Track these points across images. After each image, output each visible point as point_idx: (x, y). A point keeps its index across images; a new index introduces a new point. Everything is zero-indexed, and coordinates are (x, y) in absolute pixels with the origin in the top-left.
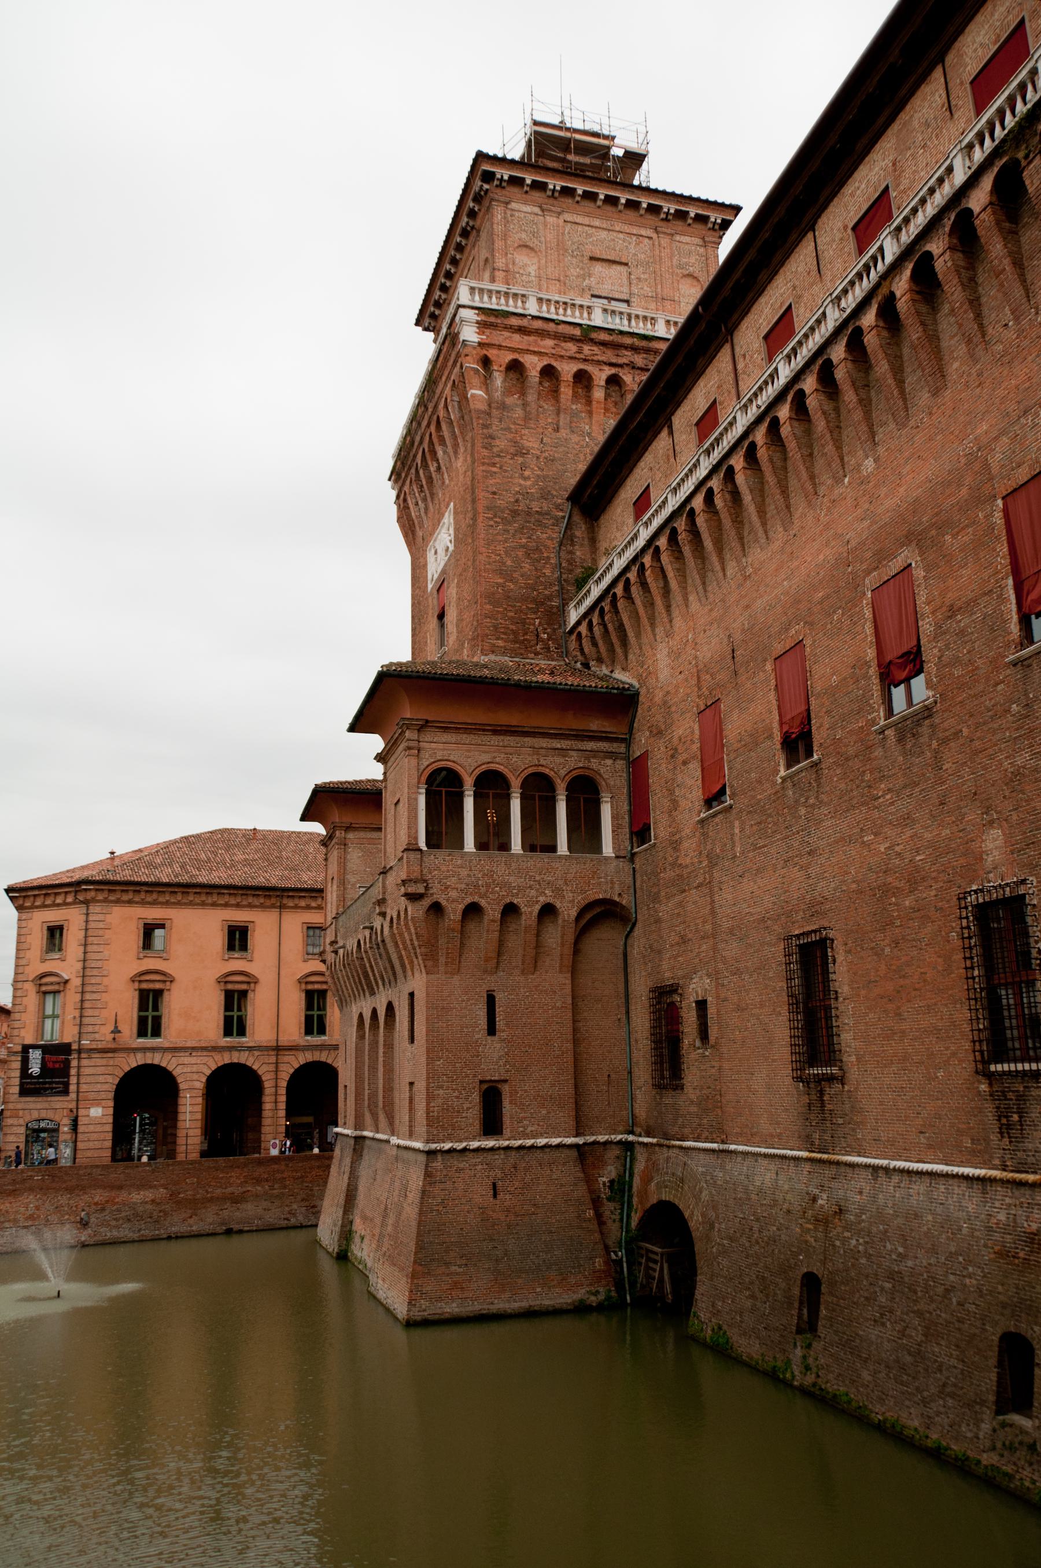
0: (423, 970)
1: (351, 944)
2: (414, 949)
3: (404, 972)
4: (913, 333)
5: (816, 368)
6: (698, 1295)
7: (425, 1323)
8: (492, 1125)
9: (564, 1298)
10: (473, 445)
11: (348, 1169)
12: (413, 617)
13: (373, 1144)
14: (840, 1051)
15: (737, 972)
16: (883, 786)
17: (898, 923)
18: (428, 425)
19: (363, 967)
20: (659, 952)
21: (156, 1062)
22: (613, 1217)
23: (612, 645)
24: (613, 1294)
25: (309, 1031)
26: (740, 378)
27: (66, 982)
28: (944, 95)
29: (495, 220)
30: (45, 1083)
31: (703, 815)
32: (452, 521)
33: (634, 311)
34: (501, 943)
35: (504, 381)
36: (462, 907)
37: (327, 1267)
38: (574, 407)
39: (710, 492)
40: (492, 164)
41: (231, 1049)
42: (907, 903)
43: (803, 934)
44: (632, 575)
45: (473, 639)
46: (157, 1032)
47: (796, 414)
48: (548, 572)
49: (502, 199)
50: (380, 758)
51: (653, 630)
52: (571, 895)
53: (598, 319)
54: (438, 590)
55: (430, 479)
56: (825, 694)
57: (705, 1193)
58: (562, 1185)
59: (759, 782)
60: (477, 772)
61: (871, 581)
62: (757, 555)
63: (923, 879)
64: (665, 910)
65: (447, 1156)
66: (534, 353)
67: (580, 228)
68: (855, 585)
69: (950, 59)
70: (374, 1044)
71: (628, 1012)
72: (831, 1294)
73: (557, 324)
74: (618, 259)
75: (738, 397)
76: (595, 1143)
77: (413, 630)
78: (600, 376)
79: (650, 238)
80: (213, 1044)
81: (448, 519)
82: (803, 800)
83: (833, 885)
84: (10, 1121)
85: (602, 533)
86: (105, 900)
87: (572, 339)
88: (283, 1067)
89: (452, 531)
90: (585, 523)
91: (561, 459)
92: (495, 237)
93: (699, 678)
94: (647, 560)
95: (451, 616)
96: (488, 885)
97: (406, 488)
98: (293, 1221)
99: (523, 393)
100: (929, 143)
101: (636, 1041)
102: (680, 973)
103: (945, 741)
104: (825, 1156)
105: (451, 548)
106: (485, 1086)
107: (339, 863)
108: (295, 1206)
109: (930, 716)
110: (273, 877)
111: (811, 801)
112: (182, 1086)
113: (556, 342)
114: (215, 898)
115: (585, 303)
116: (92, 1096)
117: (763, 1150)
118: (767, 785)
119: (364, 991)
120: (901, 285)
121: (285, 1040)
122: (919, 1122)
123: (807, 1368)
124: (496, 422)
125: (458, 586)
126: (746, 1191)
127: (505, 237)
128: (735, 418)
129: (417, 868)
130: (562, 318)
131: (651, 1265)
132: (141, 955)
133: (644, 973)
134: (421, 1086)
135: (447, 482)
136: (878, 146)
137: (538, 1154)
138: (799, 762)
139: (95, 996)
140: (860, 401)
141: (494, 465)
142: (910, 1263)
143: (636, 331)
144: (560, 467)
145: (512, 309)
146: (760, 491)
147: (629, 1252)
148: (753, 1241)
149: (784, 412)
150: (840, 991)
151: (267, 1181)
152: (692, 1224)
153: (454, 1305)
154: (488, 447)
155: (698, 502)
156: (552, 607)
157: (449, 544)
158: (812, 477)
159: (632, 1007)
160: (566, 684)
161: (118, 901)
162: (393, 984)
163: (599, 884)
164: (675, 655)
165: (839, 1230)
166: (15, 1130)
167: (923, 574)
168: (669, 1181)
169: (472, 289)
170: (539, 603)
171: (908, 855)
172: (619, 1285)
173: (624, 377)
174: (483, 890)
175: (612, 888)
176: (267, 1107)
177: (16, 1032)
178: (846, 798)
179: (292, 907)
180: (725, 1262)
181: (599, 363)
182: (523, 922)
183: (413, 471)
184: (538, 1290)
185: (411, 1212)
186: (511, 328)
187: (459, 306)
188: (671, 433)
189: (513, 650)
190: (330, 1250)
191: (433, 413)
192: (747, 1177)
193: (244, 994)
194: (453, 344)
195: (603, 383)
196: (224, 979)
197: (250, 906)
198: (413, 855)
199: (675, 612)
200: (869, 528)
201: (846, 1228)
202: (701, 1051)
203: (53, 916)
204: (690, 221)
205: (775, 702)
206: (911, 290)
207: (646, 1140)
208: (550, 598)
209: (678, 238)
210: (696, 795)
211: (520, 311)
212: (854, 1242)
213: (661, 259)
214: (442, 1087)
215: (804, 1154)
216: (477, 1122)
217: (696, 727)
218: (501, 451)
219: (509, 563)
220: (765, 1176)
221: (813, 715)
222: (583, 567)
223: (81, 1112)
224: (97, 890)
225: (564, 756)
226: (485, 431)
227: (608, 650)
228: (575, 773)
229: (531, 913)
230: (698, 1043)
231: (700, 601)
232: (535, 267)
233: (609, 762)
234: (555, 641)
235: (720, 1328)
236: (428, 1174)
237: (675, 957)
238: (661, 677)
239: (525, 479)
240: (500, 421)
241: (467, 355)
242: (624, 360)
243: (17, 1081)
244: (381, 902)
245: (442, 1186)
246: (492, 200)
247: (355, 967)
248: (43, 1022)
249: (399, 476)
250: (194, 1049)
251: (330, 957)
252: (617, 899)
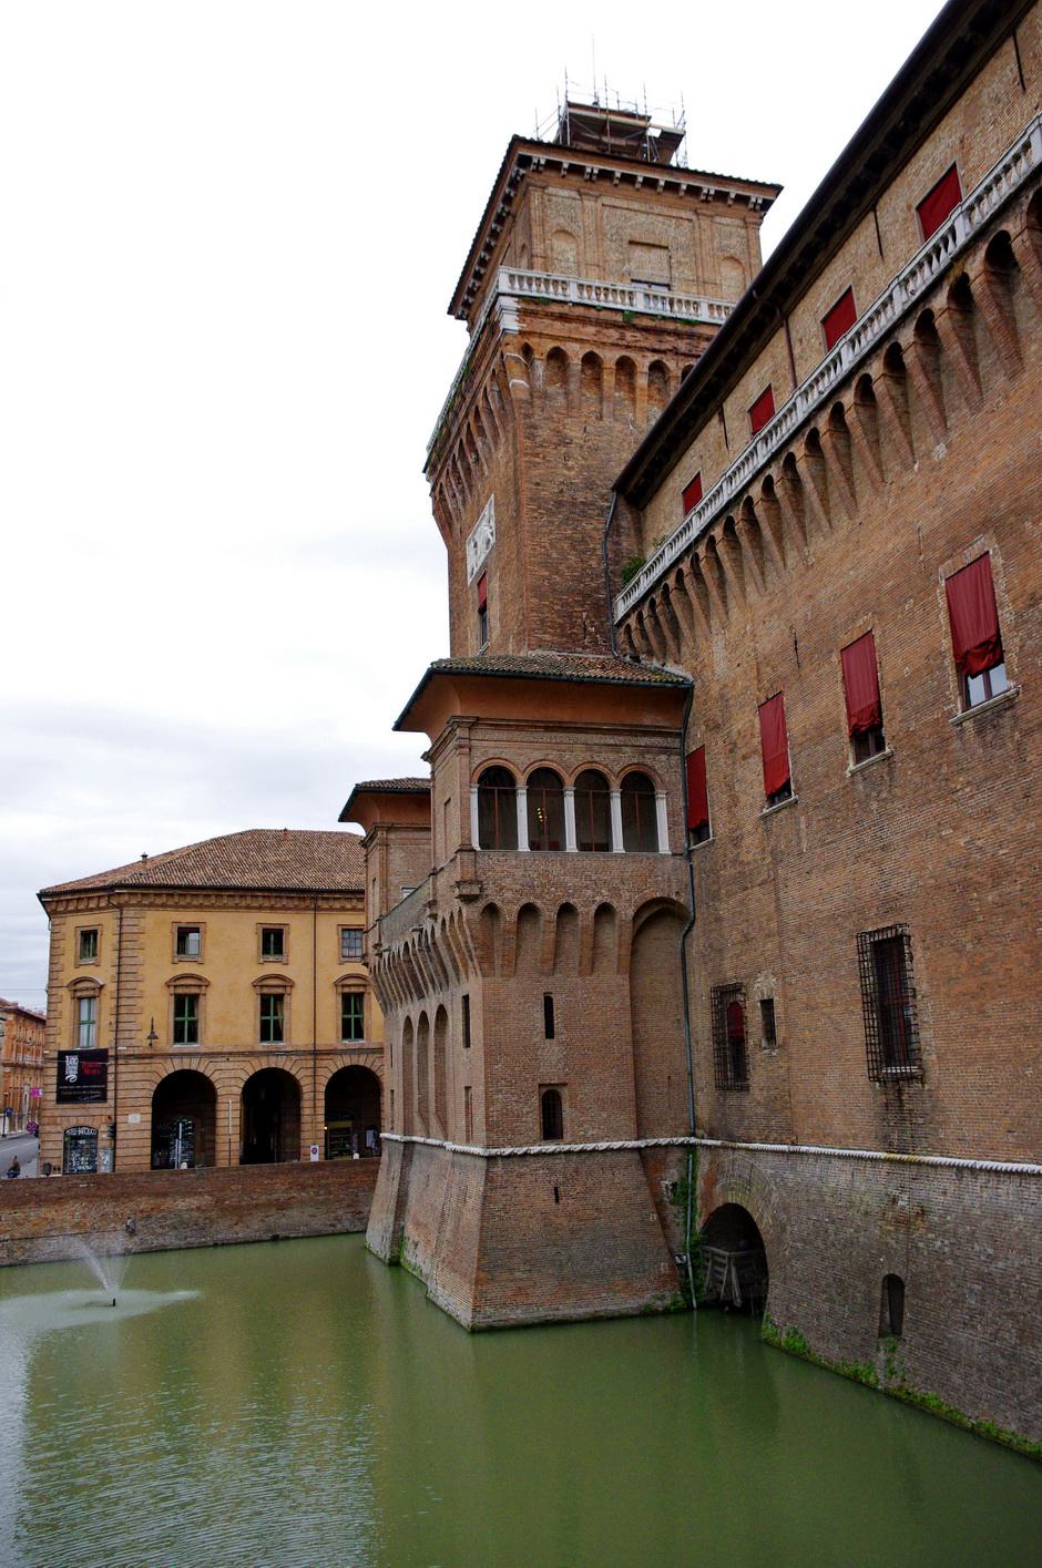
0: (479, 972)
1: (398, 946)
2: (469, 951)
3: (457, 975)
4: (988, 315)
5: (883, 352)
6: (770, 1299)
7: (491, 1330)
8: (552, 1130)
9: (631, 1304)
10: (515, 435)
11: (397, 1175)
12: (451, 611)
13: (424, 1149)
14: (919, 1049)
15: (806, 971)
16: (961, 779)
17: (981, 918)
18: (466, 416)
19: (411, 970)
20: (720, 951)
21: (194, 1067)
22: (677, 1220)
23: (664, 637)
24: (680, 1298)
25: (346, 1035)
26: (797, 364)
27: (102, 987)
28: (1016, 69)
29: (533, 206)
30: (81, 1090)
31: (765, 811)
32: (493, 513)
33: (677, 295)
34: (558, 943)
35: (546, 369)
36: (517, 908)
37: (379, 1275)
38: (617, 394)
39: (769, 480)
40: (529, 148)
41: (268, 1053)
42: (990, 898)
43: (878, 931)
44: (685, 566)
45: (519, 634)
46: (193, 1038)
47: (861, 400)
48: (594, 563)
49: (539, 183)
50: (427, 757)
51: (708, 623)
52: (628, 894)
53: (640, 305)
54: (479, 585)
55: (468, 470)
56: (896, 685)
57: (774, 1195)
58: (624, 1189)
59: (827, 776)
60: (530, 770)
61: (945, 570)
62: (819, 544)
63: (1008, 874)
64: (724, 909)
65: (509, 1161)
66: (576, 340)
67: (619, 212)
68: (928, 573)
69: (1022, 31)
70: (423, 1048)
71: (687, 1012)
72: (915, 1296)
73: (599, 310)
74: (657, 243)
75: (796, 386)
76: (656, 1146)
77: (452, 625)
78: (643, 362)
79: (690, 220)
80: (249, 1049)
81: (489, 511)
82: (874, 794)
83: (908, 880)
84: (48, 1128)
85: (648, 524)
86: (140, 904)
87: (614, 325)
88: (320, 1072)
89: (493, 524)
90: (631, 513)
91: (604, 448)
92: (533, 223)
93: (758, 670)
94: (701, 550)
95: (494, 610)
96: (543, 886)
97: (443, 480)
98: (339, 1226)
99: (565, 381)
100: (999, 119)
101: (697, 1042)
102: (743, 972)
103: (1028, 733)
104: (905, 1157)
105: (493, 540)
106: (544, 1090)
107: (381, 865)
108: (340, 1212)
109: (1012, 707)
110: (307, 879)
111: (884, 795)
112: (219, 1092)
113: (597, 329)
114: (249, 901)
115: (627, 289)
116: (130, 1102)
117: (837, 1151)
118: (834, 780)
119: (411, 993)
120: (975, 266)
121: (323, 1043)
122: (1007, 1121)
123: (892, 1372)
124: (538, 411)
125: (501, 579)
126: (820, 1193)
127: (543, 223)
128: (794, 404)
129: (472, 870)
130: (603, 304)
131: (718, 1268)
132: (176, 960)
133: (703, 973)
134: (479, 1090)
135: (486, 473)
136: (943, 123)
137: (599, 1158)
138: (869, 755)
139: (131, 1002)
140: (931, 386)
141: (537, 455)
142: (1001, 1265)
143: (679, 316)
144: (603, 457)
145: (552, 296)
146: (822, 478)
147: (695, 1256)
148: (829, 1243)
149: (848, 398)
150: (918, 988)
151: (312, 1186)
152: (761, 1227)
153: (519, 1311)
154: (531, 437)
155: (756, 491)
156: (600, 599)
157: (490, 537)
158: (879, 465)
159: (692, 1008)
160: (619, 679)
161: (151, 905)
162: (444, 987)
163: (656, 882)
164: (732, 647)
165: (922, 1231)
166: (53, 1137)
167: (1002, 561)
168: (736, 1183)
169: (512, 277)
170: (586, 596)
171: (989, 849)
172: (685, 1290)
173: (668, 363)
174: (538, 890)
175: (669, 886)
176: (306, 1112)
177: (51, 1039)
178: (921, 792)
179: (327, 910)
180: (798, 1265)
181: (642, 349)
182: (580, 923)
183: (450, 462)
184: (603, 1295)
185: (472, 1217)
186: (552, 316)
187: (499, 294)
188: (722, 420)
189: (560, 644)
190: (382, 1256)
191: (471, 404)
192: (820, 1178)
193: (279, 998)
194: (493, 332)
195: (646, 370)
196: (259, 983)
197: (285, 908)
198: (466, 856)
199: (732, 603)
200: (941, 515)
201: (929, 1230)
202: (767, 1051)
203: (87, 921)
204: (730, 202)
205: (842, 696)
206: (985, 271)
207: (709, 1142)
208: (597, 590)
209: (718, 219)
210: (759, 790)
211: (561, 298)
212: (939, 1243)
213: (701, 242)
214: (499, 1091)
215: (883, 1155)
216: (538, 1126)
217: (757, 721)
218: (544, 441)
219: (554, 555)
220: (839, 1177)
221: (884, 707)
222: (629, 558)
223: (120, 1119)
224: (130, 894)
225: (618, 752)
226: (528, 421)
227: (659, 643)
228: (628, 770)
229: (587, 913)
230: (764, 1044)
231: (759, 592)
232: (574, 253)
233: (663, 757)
234: (602, 634)
235: (796, 1332)
236: (488, 1179)
237: (738, 956)
238: (718, 670)
239: (569, 469)
240: (543, 411)
241: (507, 344)
242: (668, 346)
243: (54, 1088)
244: (432, 904)
245: (503, 1191)
246: (528, 185)
247: (402, 970)
248: (79, 1028)
249: (434, 467)
250: (230, 1053)
251: (373, 960)
252: (674, 897)
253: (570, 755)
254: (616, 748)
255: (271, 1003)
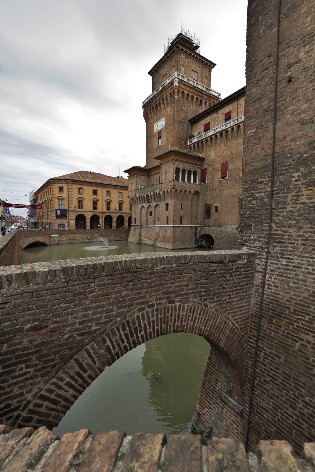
9: (190, 247)
41: (95, 212)
46: (82, 208)
78: (195, 97)
86: (72, 183)
99: (183, 98)
121: (103, 211)
154: (178, 108)
161: (74, 184)
197: (97, 187)
203: (60, 185)
253: (187, 167)
254: (193, 167)
255: (95, 203)
